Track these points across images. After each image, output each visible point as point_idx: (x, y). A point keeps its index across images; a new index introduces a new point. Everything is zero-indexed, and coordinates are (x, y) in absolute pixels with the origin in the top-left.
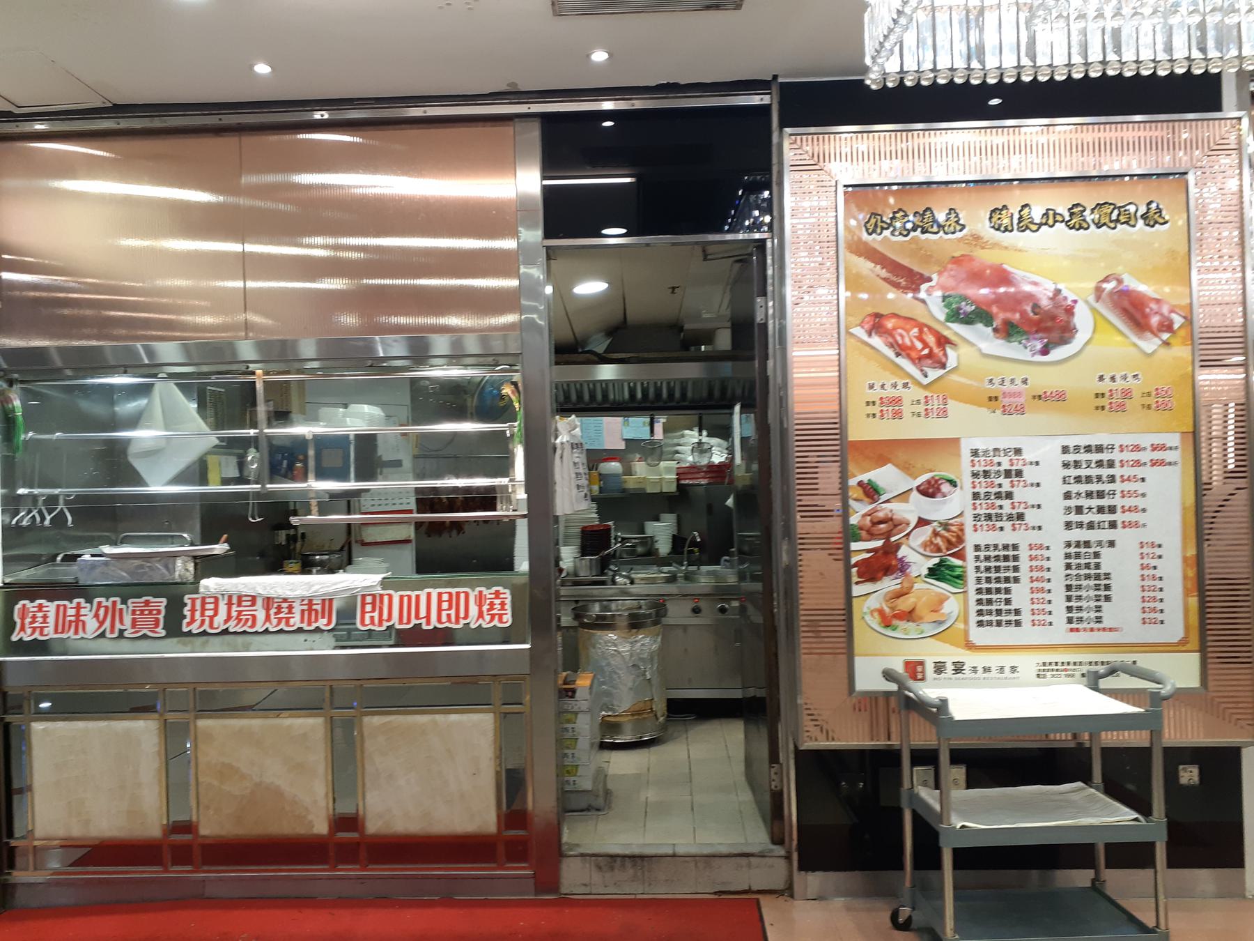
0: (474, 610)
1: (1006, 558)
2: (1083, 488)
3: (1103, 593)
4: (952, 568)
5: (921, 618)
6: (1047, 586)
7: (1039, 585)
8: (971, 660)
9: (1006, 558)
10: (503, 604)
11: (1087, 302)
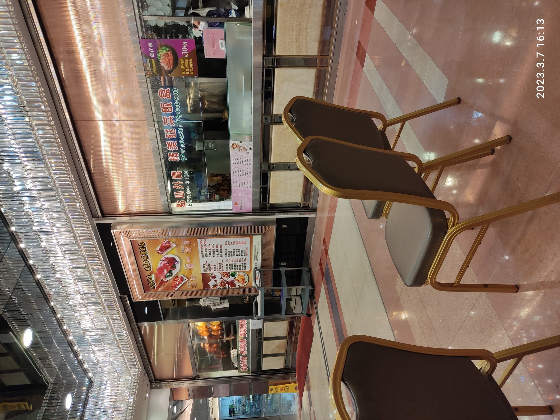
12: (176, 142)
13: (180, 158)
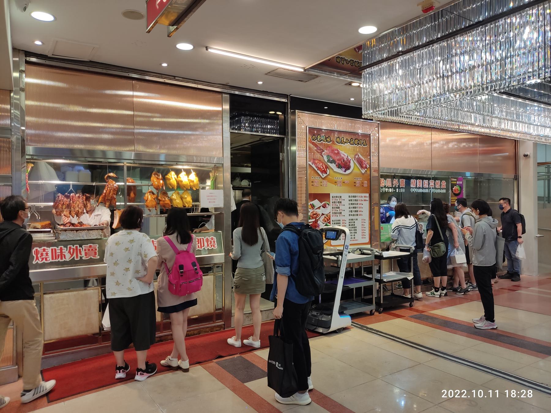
0: (206, 244)
10: (214, 242)
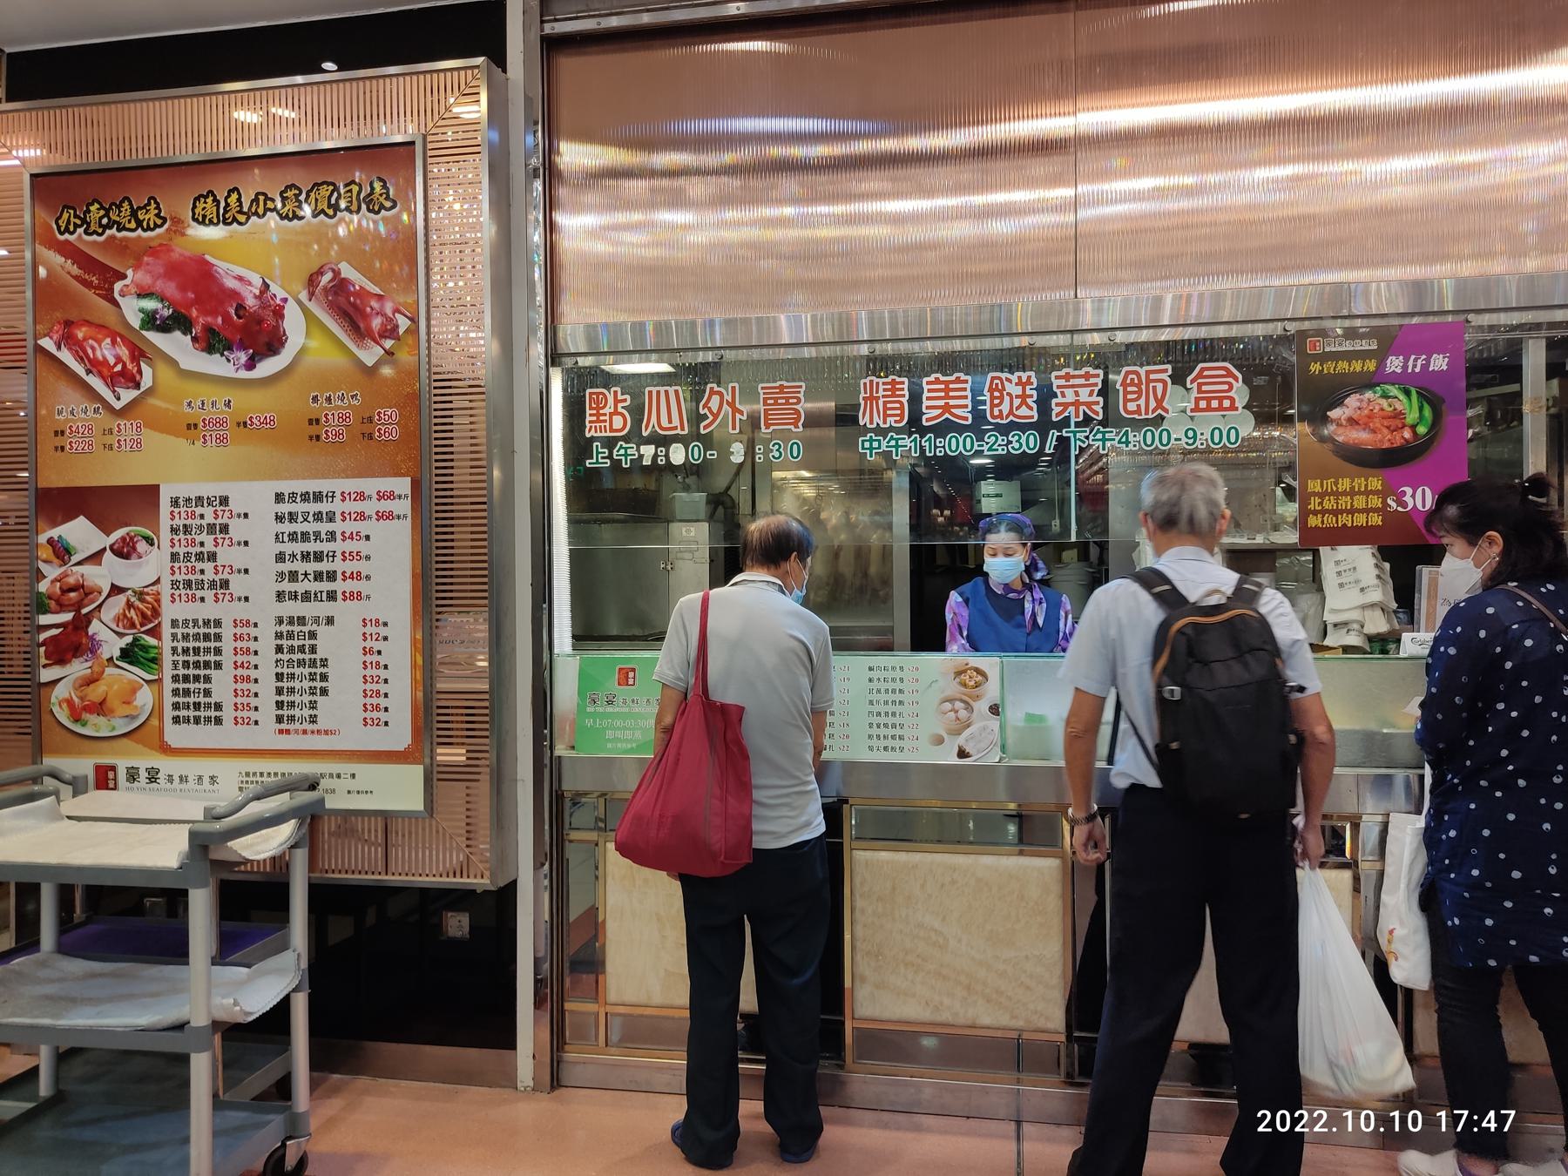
1: (207, 637)
2: (299, 548)
3: (318, 684)
4: (145, 648)
5: (112, 711)
6: (253, 674)
7: (245, 672)
8: (166, 765)
9: (207, 637)
11: (300, 303)
12: (964, 415)
13: (880, 431)
